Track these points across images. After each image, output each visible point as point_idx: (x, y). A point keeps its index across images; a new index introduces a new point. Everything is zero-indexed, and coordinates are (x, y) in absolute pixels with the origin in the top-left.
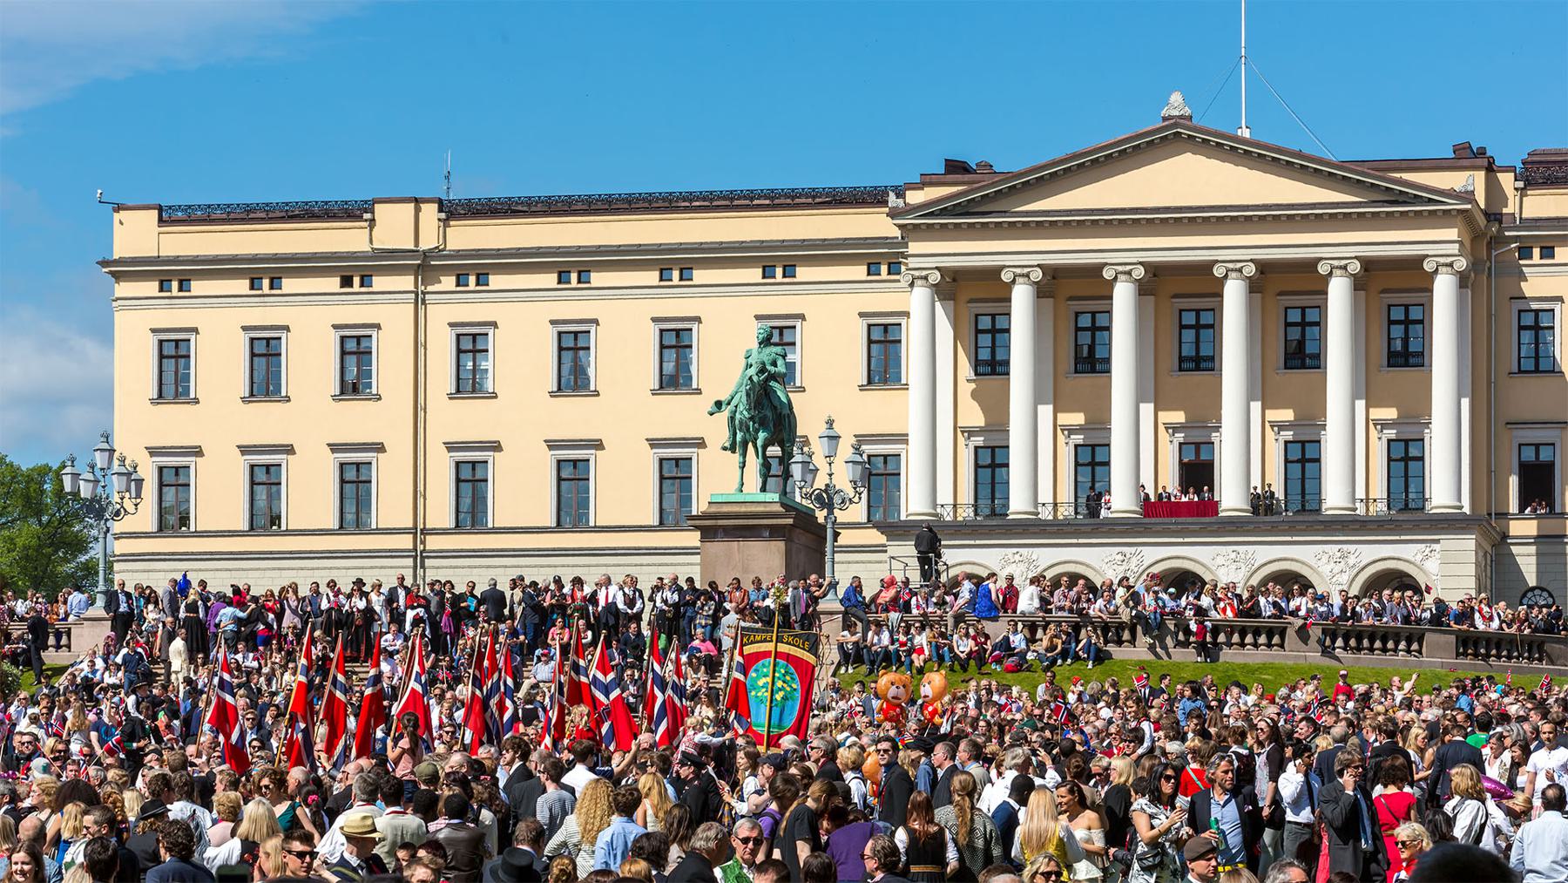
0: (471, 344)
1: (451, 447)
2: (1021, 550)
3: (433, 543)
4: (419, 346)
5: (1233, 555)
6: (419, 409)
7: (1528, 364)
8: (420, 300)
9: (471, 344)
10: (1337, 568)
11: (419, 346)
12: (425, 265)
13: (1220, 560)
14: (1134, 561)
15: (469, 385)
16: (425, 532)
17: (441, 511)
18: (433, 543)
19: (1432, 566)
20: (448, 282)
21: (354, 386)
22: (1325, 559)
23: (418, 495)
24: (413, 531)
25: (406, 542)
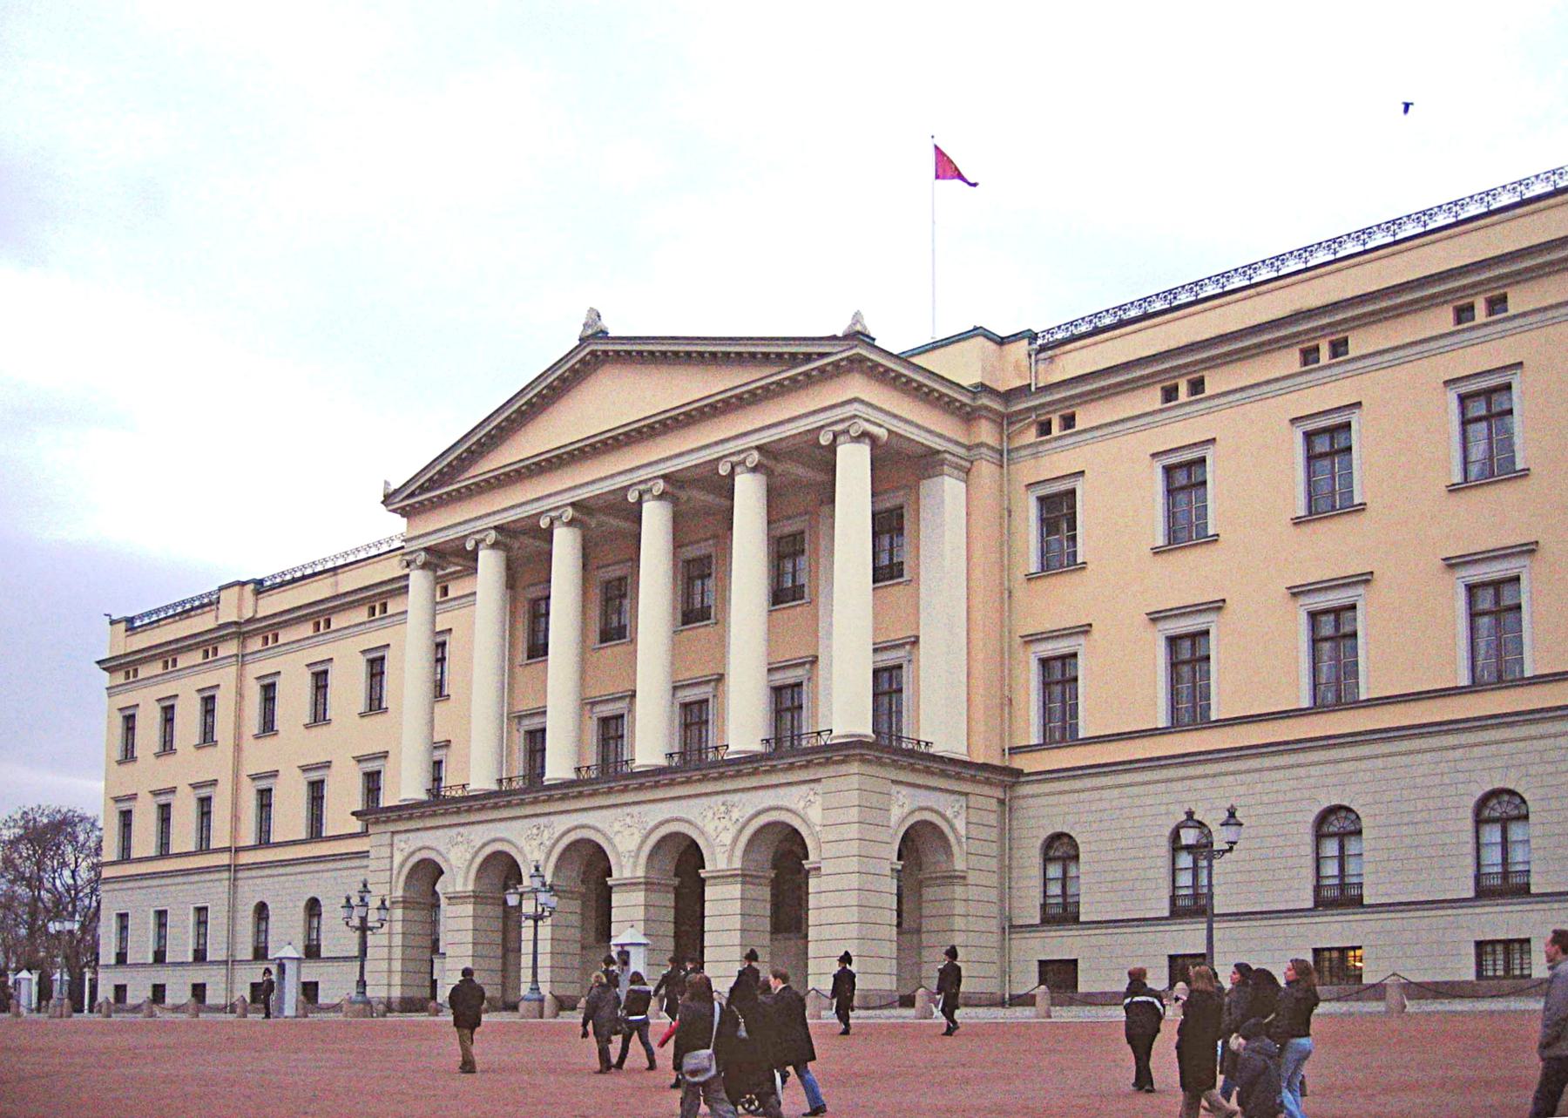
1: (255, 778)
2: (461, 829)
3: (245, 858)
4: (240, 695)
5: (628, 820)
6: (238, 748)
8: (242, 659)
11: (240, 695)
15: (268, 725)
16: (238, 850)
18: (245, 858)
19: (815, 814)
22: (710, 814)
23: (235, 818)
24: (228, 849)
25: (224, 859)
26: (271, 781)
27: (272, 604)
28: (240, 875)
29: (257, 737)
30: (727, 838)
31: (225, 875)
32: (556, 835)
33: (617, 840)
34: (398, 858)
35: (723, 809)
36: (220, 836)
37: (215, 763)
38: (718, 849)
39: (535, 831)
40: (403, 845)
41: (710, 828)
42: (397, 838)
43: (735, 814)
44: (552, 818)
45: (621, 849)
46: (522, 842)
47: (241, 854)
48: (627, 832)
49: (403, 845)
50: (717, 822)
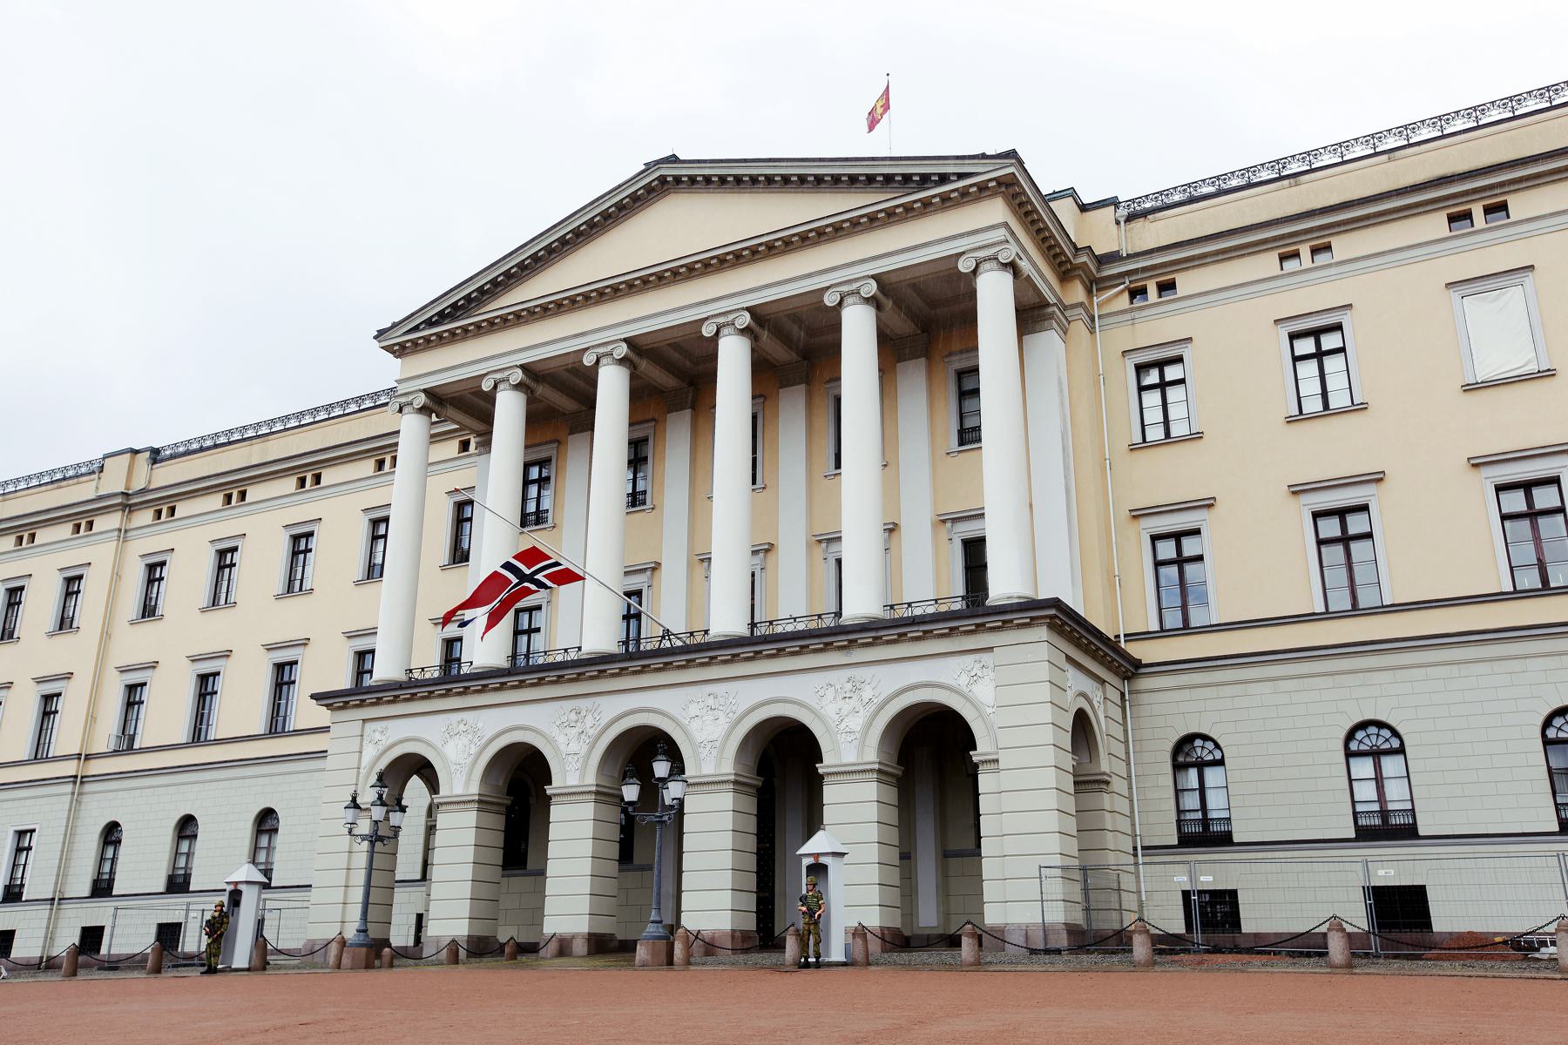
0: (154, 572)
3: (96, 767)
4: (117, 576)
5: (710, 701)
6: (106, 635)
7: (1155, 434)
8: (123, 534)
9: (154, 572)
10: (847, 706)
11: (117, 576)
12: (127, 503)
13: (694, 709)
14: (589, 721)
16: (88, 757)
17: (106, 734)
19: (984, 692)
20: (146, 516)
21: (65, 623)
22: (830, 693)
23: (91, 719)
25: (70, 768)
26: (149, 673)
27: (167, 475)
28: (88, 788)
29: (132, 623)
30: (856, 723)
31: (69, 788)
32: (604, 722)
33: (694, 727)
34: (370, 753)
35: (849, 686)
36: (66, 737)
37: (74, 653)
38: (842, 738)
39: (573, 716)
40: (377, 736)
41: (830, 709)
42: (370, 726)
43: (867, 693)
44: (598, 700)
45: (699, 737)
46: (554, 732)
47: (92, 762)
48: (709, 717)
49: (377, 736)
50: (841, 703)
